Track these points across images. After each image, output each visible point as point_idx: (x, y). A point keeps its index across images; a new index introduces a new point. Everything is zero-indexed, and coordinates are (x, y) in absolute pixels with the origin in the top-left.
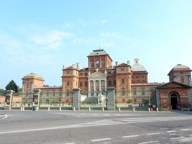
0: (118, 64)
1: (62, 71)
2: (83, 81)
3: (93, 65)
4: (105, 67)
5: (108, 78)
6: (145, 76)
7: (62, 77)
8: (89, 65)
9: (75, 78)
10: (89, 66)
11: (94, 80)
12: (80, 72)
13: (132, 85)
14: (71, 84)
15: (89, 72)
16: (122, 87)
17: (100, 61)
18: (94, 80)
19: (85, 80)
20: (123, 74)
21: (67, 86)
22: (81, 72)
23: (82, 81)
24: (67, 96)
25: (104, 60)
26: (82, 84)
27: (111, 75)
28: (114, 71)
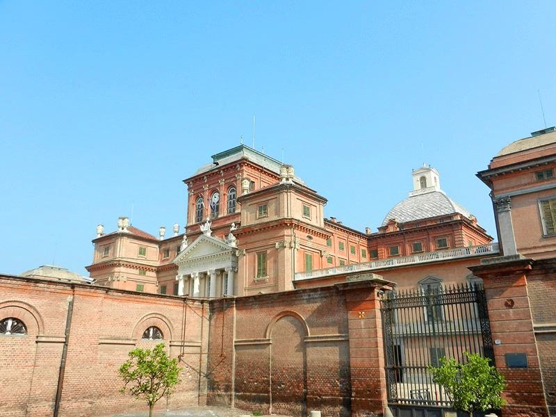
1: (92, 246)
9: (122, 269)
11: (195, 273)
12: (163, 247)
17: (222, 192)
18: (195, 273)
23: (166, 279)
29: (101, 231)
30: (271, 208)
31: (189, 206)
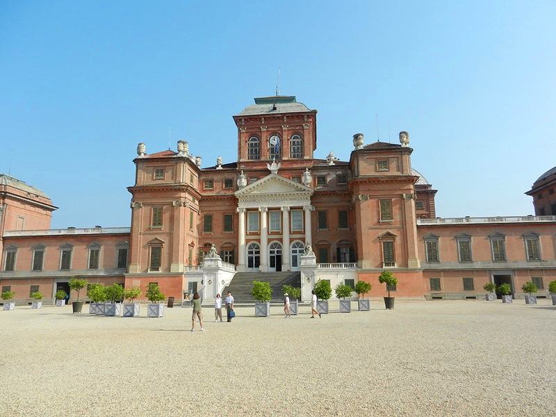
0: (365, 142)
2: (218, 211)
3: (256, 151)
4: (305, 158)
5: (315, 197)
6: (428, 201)
7: (130, 189)
8: (240, 149)
9: (187, 195)
10: (240, 153)
11: (263, 206)
13: (419, 223)
14: (172, 219)
15: (242, 175)
16: (385, 232)
17: (285, 137)
18: (263, 206)
19: (223, 208)
20: (387, 181)
21: (154, 224)
22: (210, 177)
23: (211, 209)
24: (153, 269)
25: (299, 133)
26: (214, 222)
27: (326, 189)
28: (339, 173)
29: (147, 151)
30: (393, 164)
31: (240, 142)
